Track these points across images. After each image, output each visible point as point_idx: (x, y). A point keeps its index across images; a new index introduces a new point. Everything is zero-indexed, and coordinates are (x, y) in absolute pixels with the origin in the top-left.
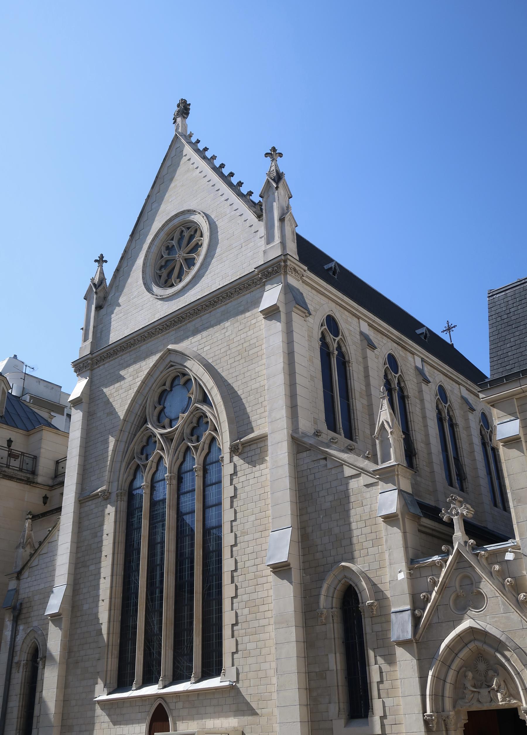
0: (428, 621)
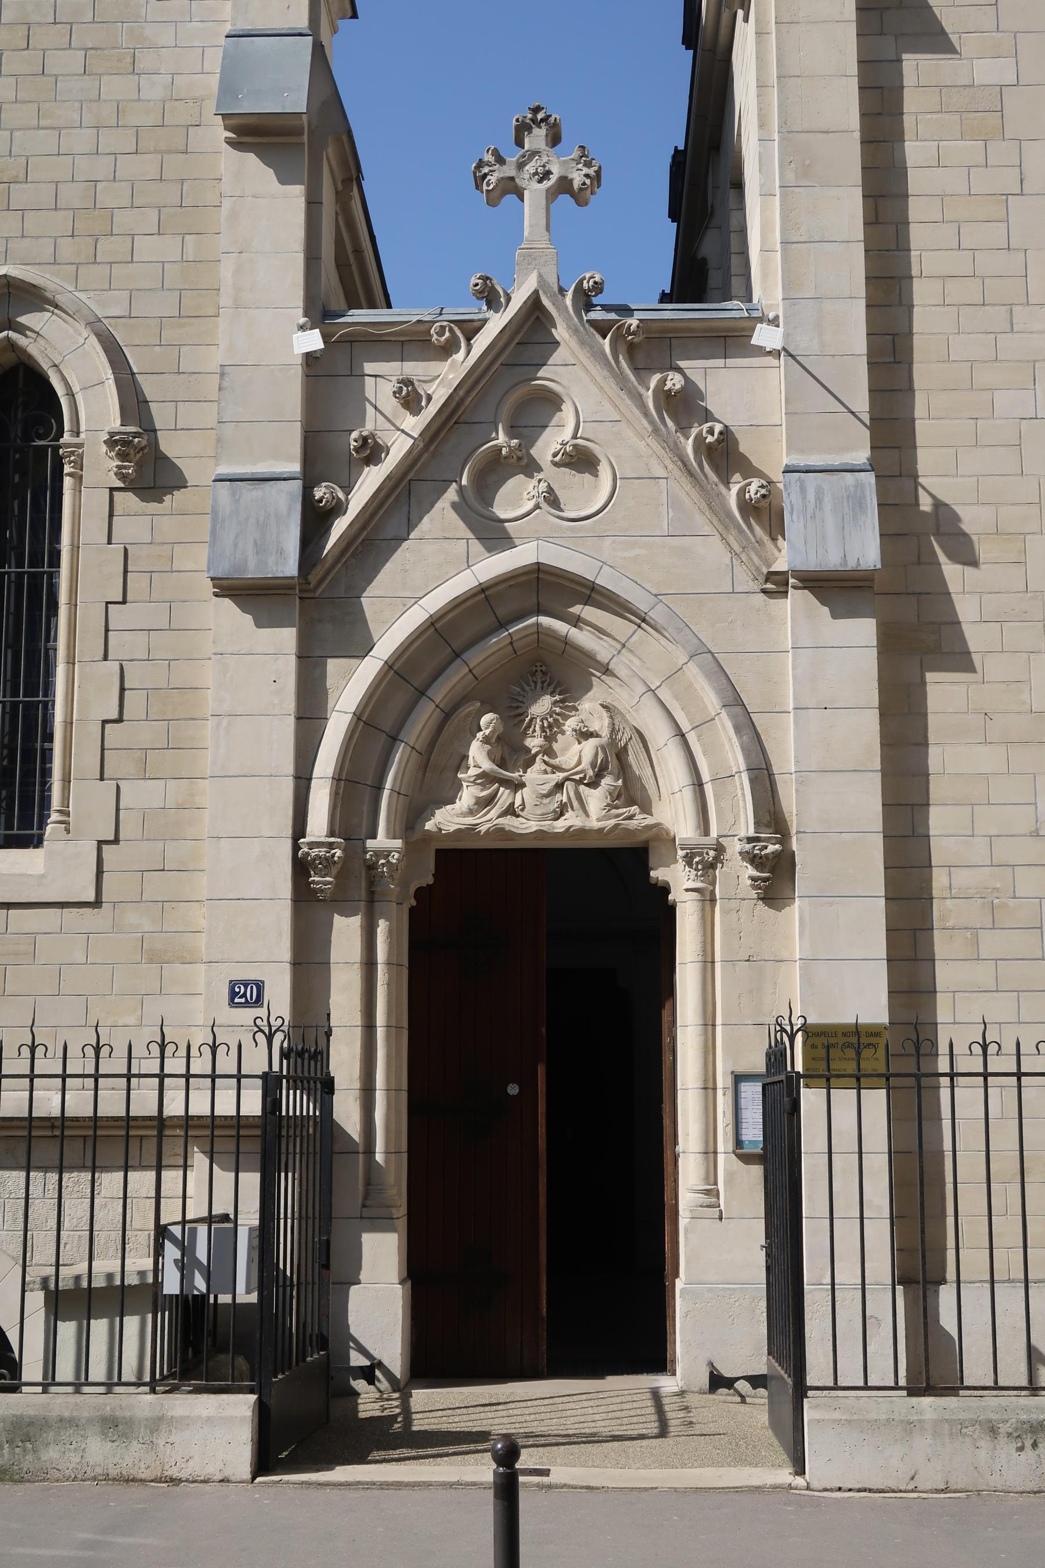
0: (363, 528)
